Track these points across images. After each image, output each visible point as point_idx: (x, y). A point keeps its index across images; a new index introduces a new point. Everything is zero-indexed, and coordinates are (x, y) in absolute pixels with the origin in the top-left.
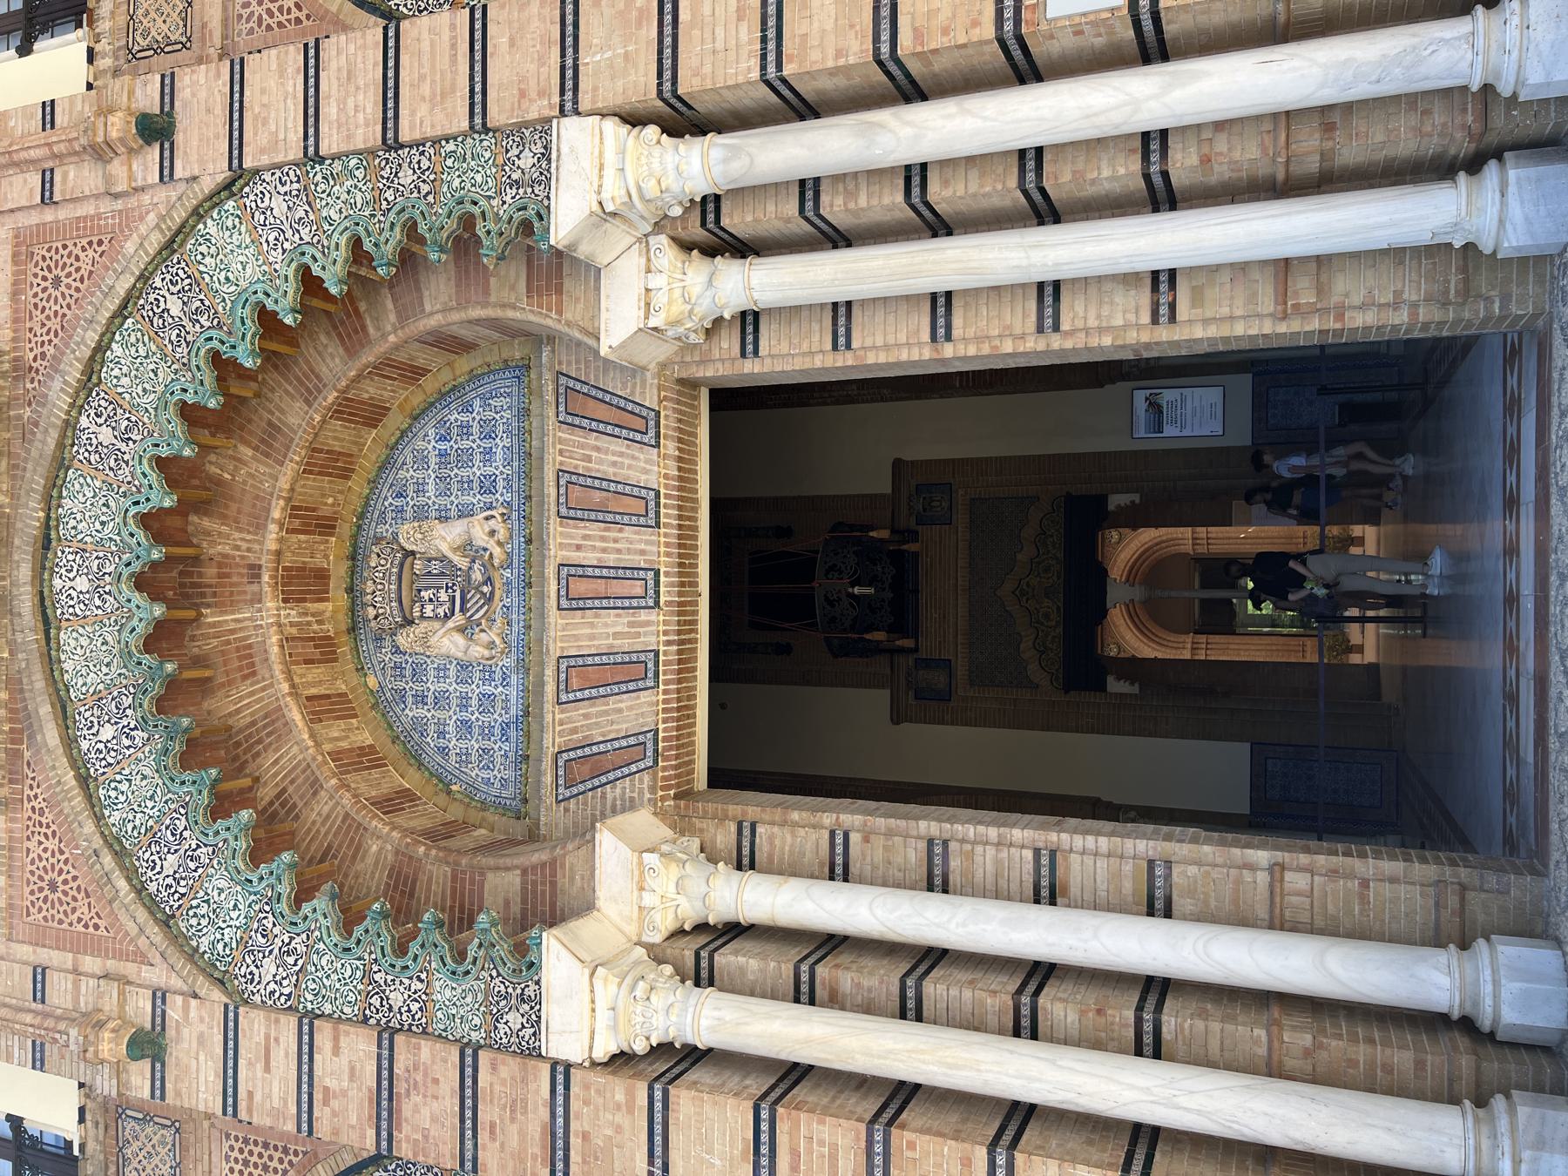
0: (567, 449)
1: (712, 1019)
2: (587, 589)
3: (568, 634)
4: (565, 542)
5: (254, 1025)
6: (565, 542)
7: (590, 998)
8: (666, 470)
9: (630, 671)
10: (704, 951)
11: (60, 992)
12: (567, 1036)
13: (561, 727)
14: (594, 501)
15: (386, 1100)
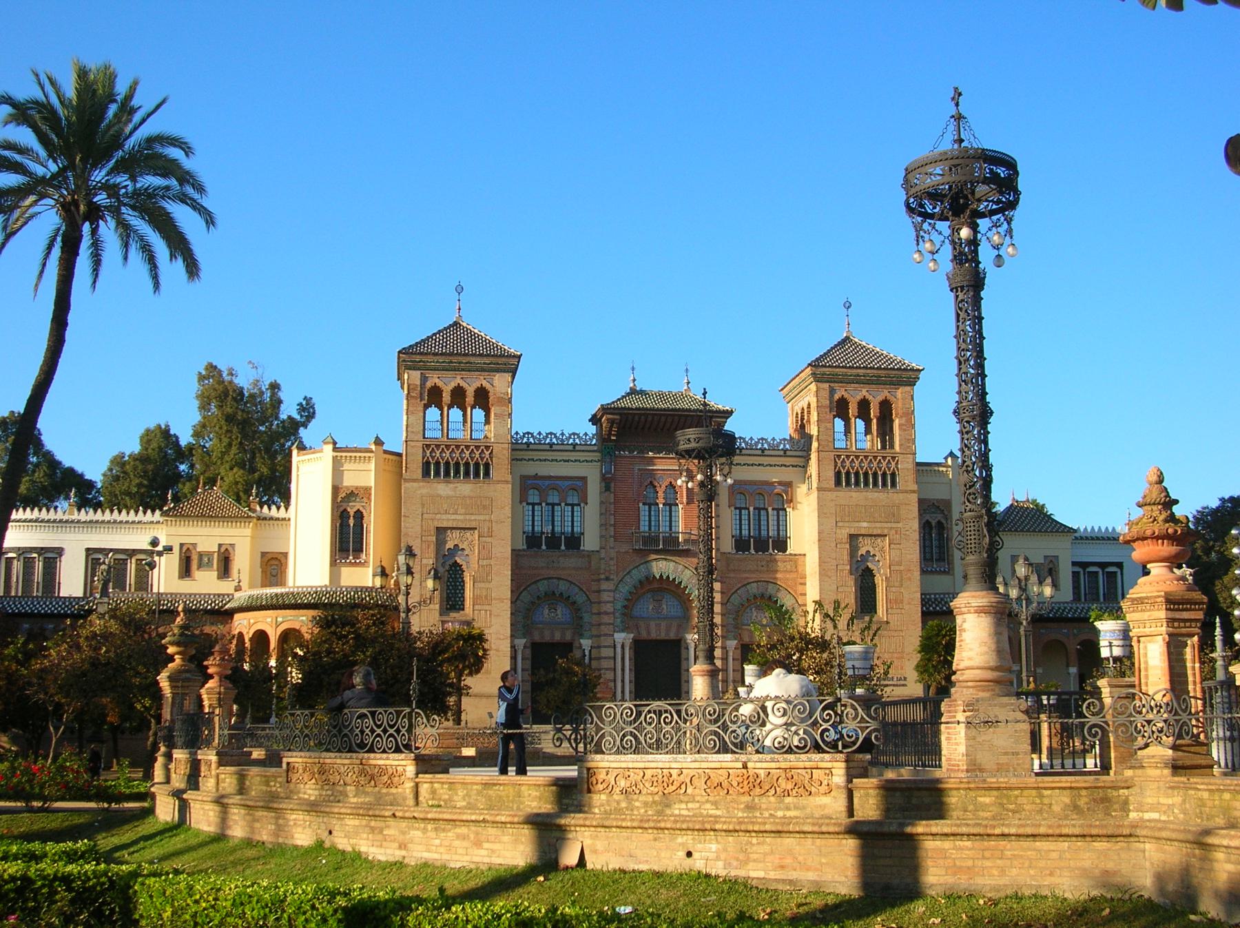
0: (675, 624)
1: (619, 650)
2: (658, 626)
3: (653, 624)
4: (663, 624)
5: (611, 594)
6: (663, 624)
7: (620, 637)
8: (672, 636)
9: (649, 633)
10: (623, 647)
11: (612, 563)
12: (616, 635)
13: (641, 623)
14: (668, 629)
15: (606, 613)
